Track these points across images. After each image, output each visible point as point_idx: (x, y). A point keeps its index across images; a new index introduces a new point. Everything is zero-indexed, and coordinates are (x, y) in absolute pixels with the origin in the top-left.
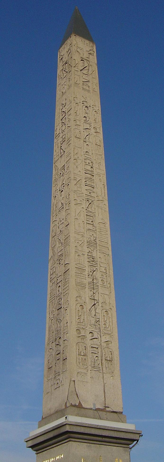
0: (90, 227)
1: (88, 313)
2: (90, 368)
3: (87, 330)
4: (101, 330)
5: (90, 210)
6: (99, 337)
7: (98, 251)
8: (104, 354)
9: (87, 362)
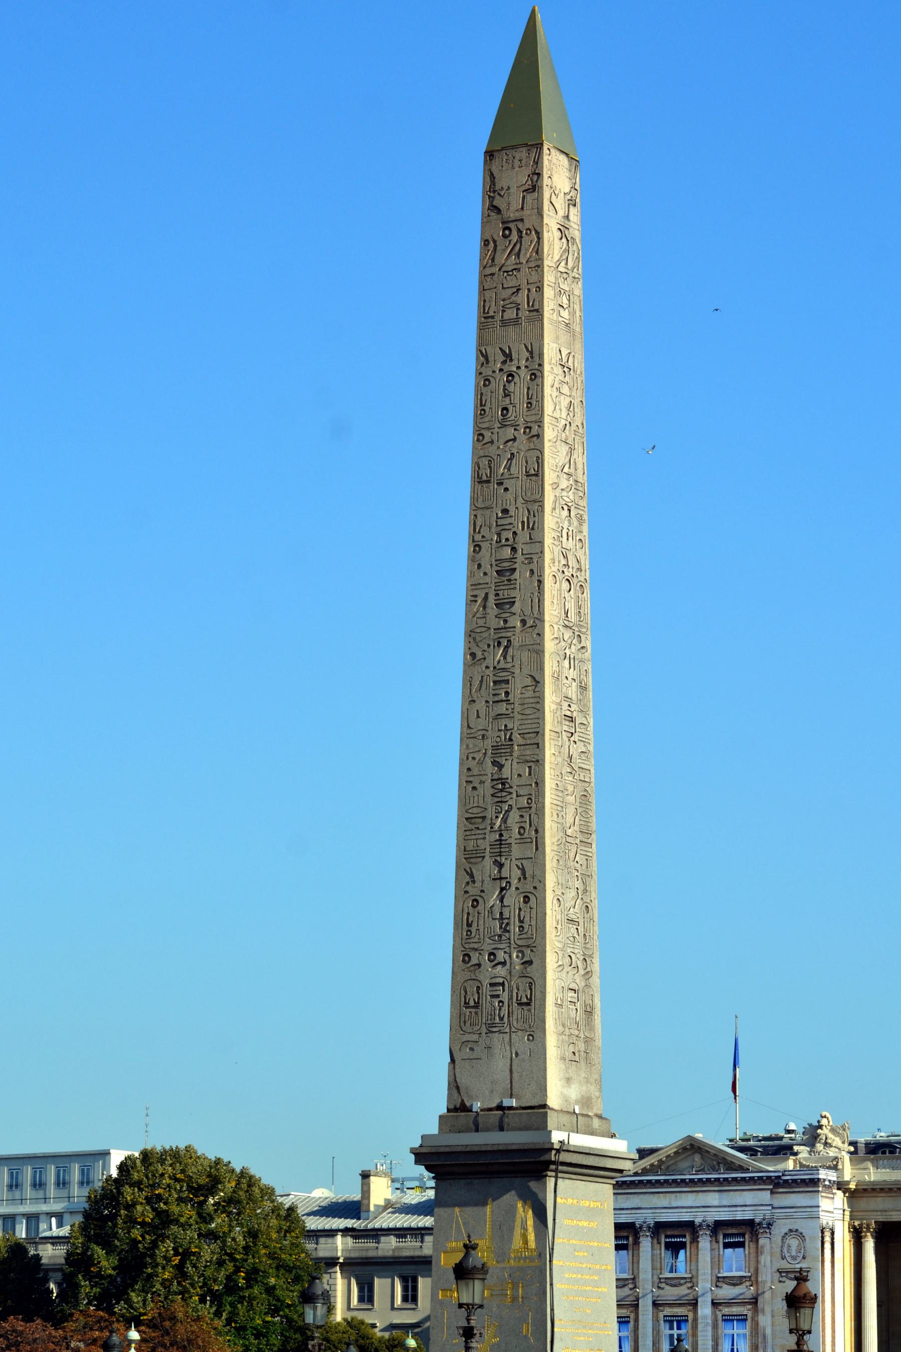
0: (502, 708)
1: (487, 913)
2: (484, 1030)
3: (483, 950)
4: (512, 942)
6: (507, 958)
7: (515, 761)
8: (515, 991)
9: (480, 1018)
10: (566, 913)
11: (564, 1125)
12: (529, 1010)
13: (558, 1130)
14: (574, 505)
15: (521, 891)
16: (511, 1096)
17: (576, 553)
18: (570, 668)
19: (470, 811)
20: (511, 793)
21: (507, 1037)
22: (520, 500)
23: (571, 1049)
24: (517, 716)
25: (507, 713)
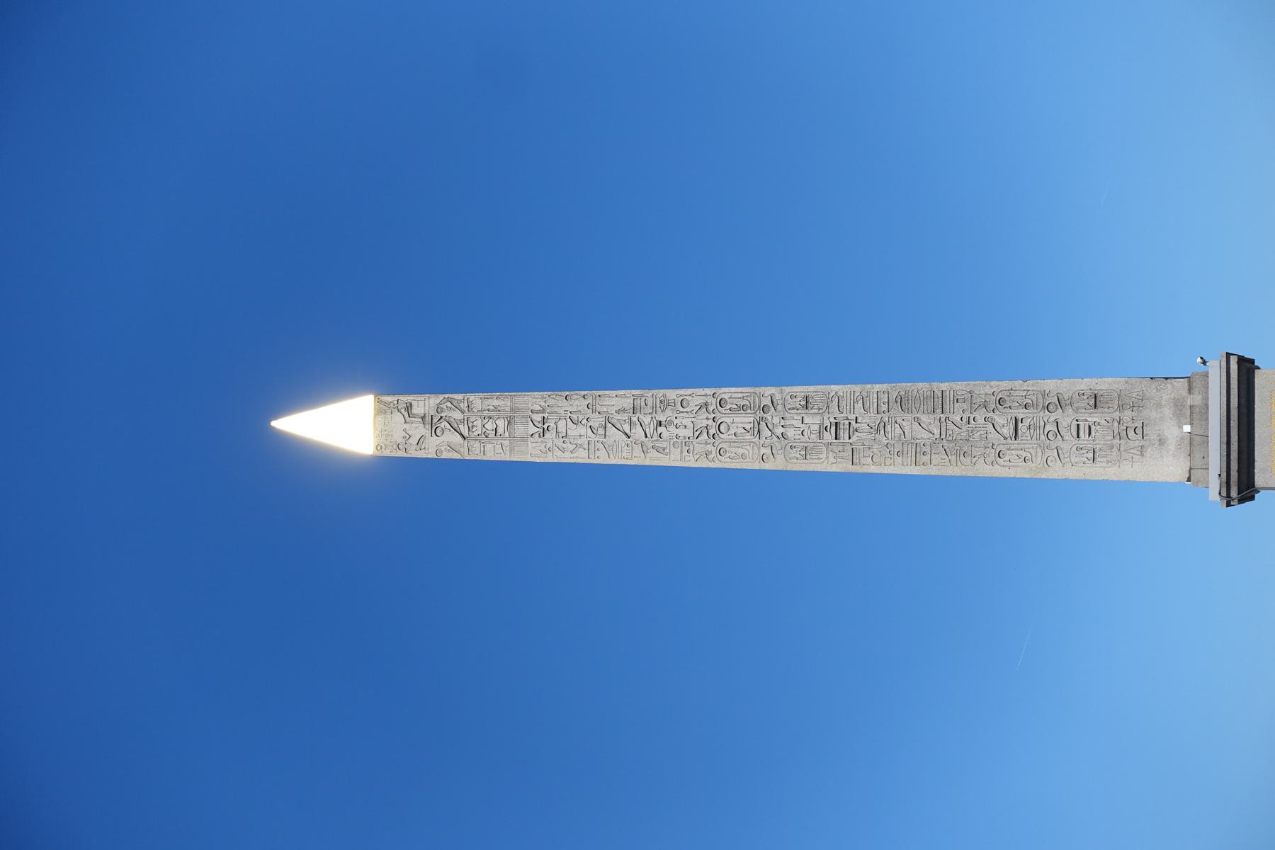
10: (1009, 441)
11: (1203, 458)
13: (1208, 469)
14: (654, 415)
17: (694, 412)
23: (1131, 433)
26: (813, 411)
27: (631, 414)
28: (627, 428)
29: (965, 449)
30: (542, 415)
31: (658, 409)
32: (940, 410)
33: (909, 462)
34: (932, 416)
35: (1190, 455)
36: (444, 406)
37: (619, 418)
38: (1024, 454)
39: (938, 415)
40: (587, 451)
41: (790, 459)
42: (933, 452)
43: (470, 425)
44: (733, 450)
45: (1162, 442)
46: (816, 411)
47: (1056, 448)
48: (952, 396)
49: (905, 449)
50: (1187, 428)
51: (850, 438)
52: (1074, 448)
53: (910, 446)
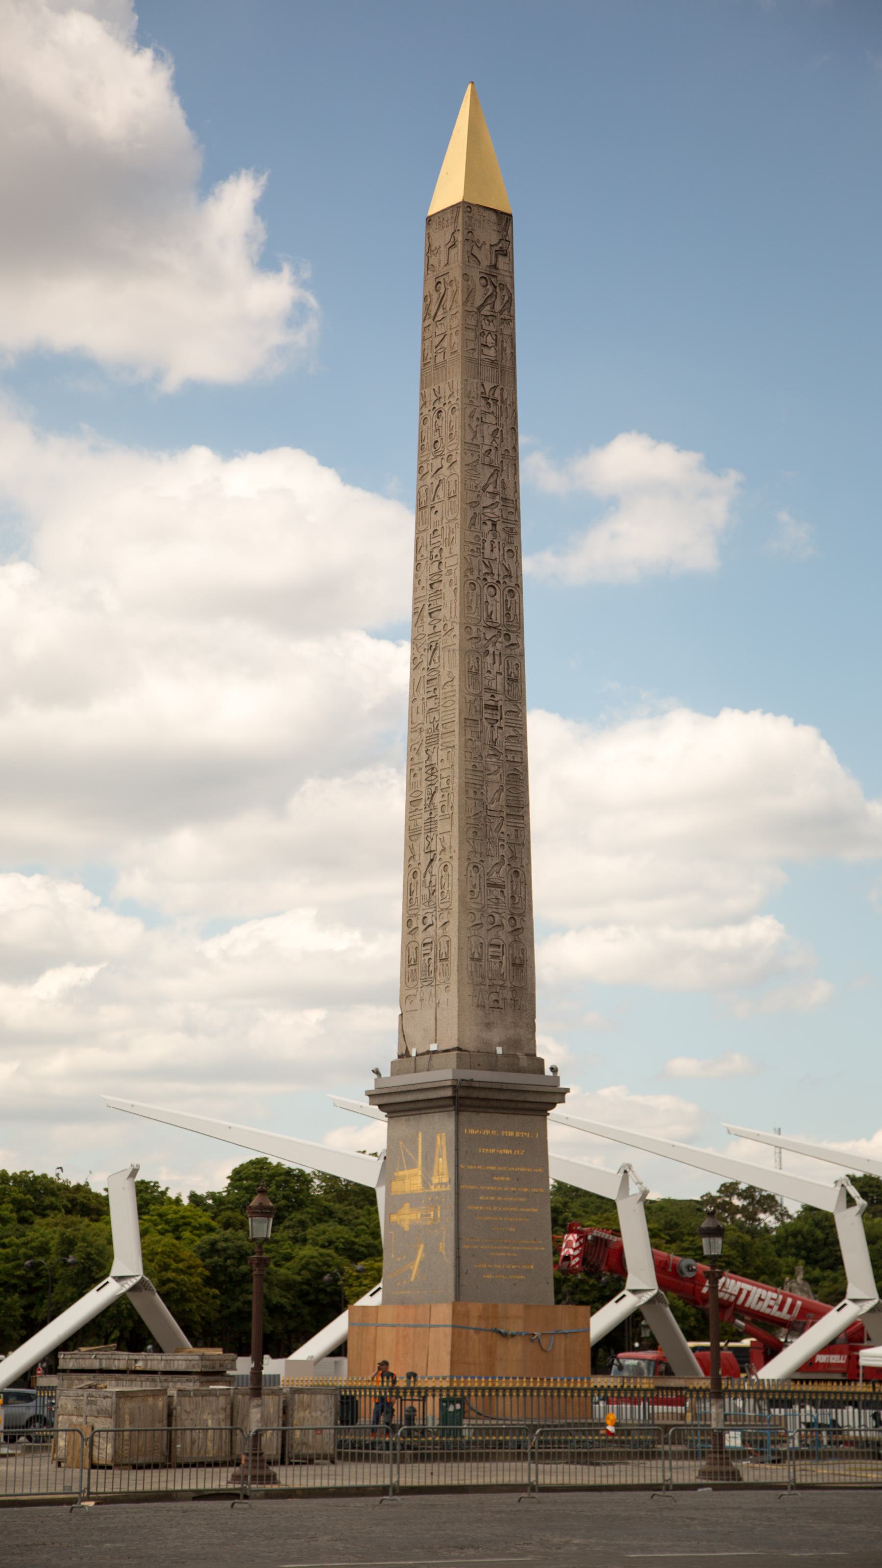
0: (431, 704)
5: (433, 666)
7: (440, 747)
8: (439, 949)
10: (486, 878)
11: (479, 1065)
12: (447, 965)
13: (471, 1069)
14: (502, 520)
15: (443, 861)
16: (436, 1042)
18: (494, 663)
19: (413, 795)
20: (437, 777)
21: (433, 989)
22: (445, 520)
23: (494, 997)
24: (442, 709)
25: (436, 706)
26: (506, 685)
27: (501, 495)
28: (490, 489)
29: (479, 834)
30: (499, 399)
31: (506, 525)
32: (509, 812)
33: (468, 776)
34: (504, 804)
35: (479, 1052)
36: (505, 293)
37: (498, 481)
38: (477, 890)
39: (506, 811)
40: (470, 441)
41: (468, 655)
42: (477, 802)
43: (490, 318)
44: (474, 598)
45: (488, 1026)
46: (507, 688)
47: (482, 923)
48: (520, 825)
49: (479, 774)
50: (499, 1050)
51: (486, 718)
52: (481, 941)
53: (481, 778)
